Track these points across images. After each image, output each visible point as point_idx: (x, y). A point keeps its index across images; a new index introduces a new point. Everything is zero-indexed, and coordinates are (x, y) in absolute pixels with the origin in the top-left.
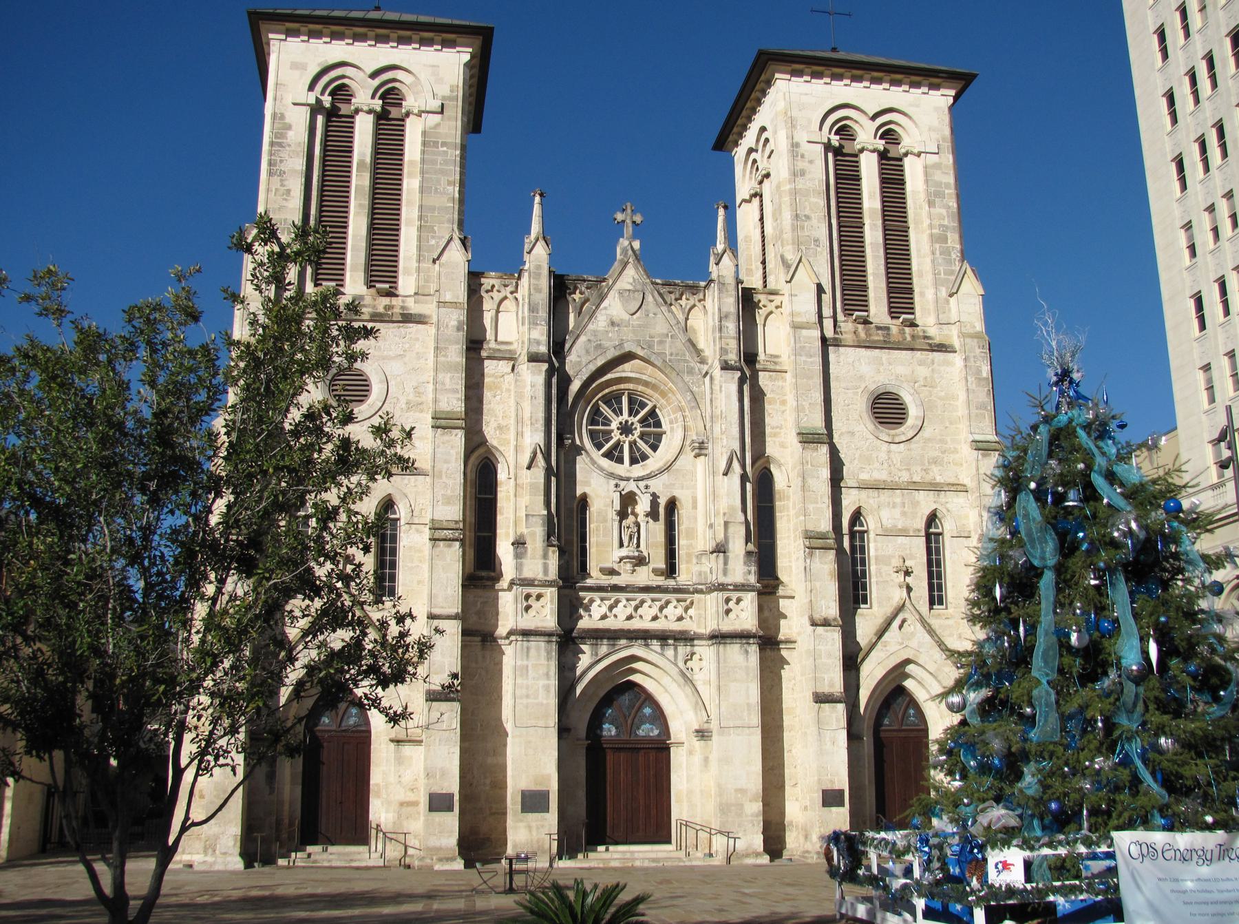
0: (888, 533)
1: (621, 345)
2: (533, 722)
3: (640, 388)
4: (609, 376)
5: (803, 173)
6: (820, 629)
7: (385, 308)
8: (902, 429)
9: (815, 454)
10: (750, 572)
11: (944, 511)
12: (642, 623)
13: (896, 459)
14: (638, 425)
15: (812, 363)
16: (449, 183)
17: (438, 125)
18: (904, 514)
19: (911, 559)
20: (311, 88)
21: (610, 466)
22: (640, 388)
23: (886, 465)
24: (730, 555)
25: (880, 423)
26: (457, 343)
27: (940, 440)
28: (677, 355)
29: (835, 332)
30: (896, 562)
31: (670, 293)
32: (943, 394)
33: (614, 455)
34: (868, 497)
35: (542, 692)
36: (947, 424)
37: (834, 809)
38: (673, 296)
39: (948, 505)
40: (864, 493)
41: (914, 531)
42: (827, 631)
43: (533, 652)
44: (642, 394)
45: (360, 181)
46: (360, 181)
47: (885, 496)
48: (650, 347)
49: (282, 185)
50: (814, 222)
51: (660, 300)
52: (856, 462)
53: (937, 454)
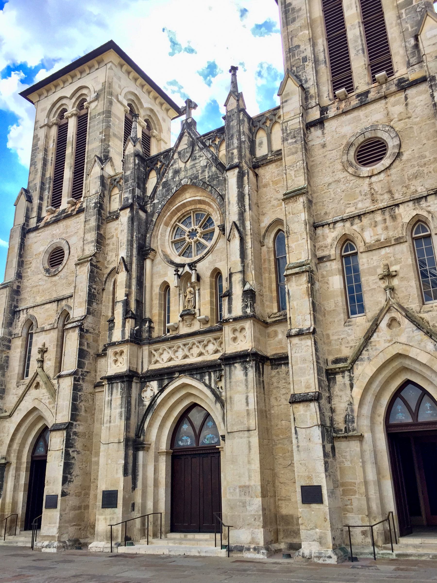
0: (370, 249)
1: (180, 183)
2: (112, 440)
3: (198, 206)
4: (178, 204)
5: (294, 20)
6: (295, 340)
7: (71, 211)
8: (382, 162)
9: (295, 205)
10: (246, 306)
11: (425, 214)
12: (193, 360)
13: (376, 187)
14: (199, 230)
15: (296, 142)
16: (101, 133)
17: (97, 105)
18: (386, 228)
19: (396, 264)
20: (48, 116)
21: (181, 260)
22: (198, 206)
23: (369, 196)
24: (233, 297)
25: (364, 165)
26: (94, 215)
27: (419, 157)
28: (212, 175)
29: (321, 114)
30: (380, 271)
31: (209, 139)
32: (418, 119)
33: (185, 253)
34: (352, 224)
35: (118, 417)
36: (425, 141)
37: (315, 506)
38: (211, 141)
39: (429, 209)
40: (348, 224)
41: (395, 240)
42: (301, 340)
43: (115, 391)
44: (201, 210)
45: (70, 151)
46: (70, 151)
47: (366, 220)
48: (196, 177)
49: (35, 168)
50: (302, 48)
51: (201, 146)
52: (342, 202)
53: (416, 168)
